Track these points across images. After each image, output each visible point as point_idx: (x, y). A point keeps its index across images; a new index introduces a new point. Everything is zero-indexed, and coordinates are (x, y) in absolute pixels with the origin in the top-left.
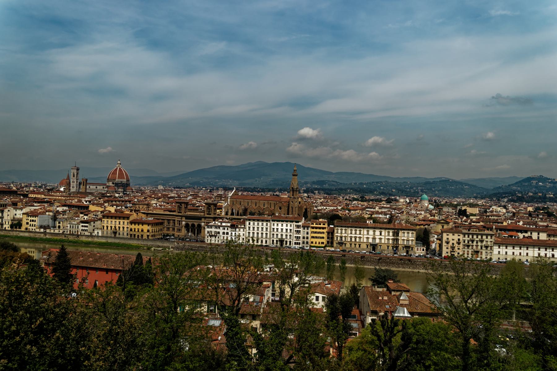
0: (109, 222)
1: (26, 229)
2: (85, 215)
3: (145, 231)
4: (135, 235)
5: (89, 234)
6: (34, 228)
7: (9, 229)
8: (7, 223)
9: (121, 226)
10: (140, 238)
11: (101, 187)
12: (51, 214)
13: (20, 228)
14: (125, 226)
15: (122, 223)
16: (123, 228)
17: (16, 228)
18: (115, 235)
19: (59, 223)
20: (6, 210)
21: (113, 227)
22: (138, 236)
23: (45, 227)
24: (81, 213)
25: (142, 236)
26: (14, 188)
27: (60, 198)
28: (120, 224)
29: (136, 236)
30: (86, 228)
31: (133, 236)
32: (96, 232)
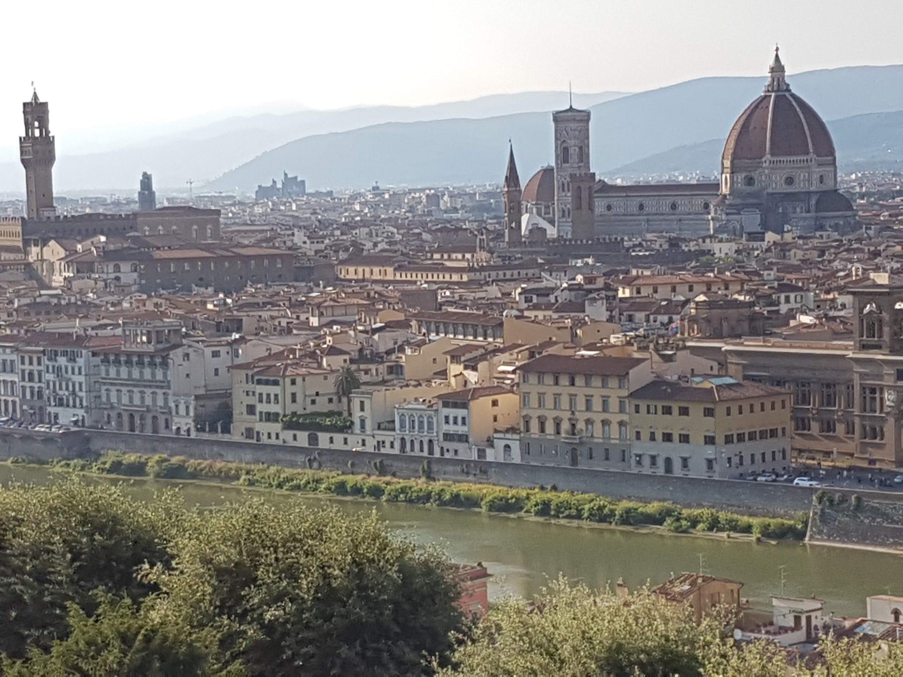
0: (549, 402)
1: (249, 432)
2: (466, 368)
3: (697, 438)
4: (653, 458)
5: (474, 456)
6: (276, 427)
7: (193, 435)
8: (182, 408)
9: (598, 418)
10: (678, 471)
11: (699, 202)
12: (338, 362)
13: (229, 432)
14: (615, 418)
15: (597, 405)
16: (605, 423)
17: (213, 430)
18: (574, 461)
19: (362, 409)
20: (176, 356)
21: (565, 426)
22: (668, 461)
23: (312, 424)
24: (455, 357)
25: (685, 461)
26: (299, 238)
27: (455, 278)
28: (588, 408)
29: (661, 462)
30: (461, 429)
31: (646, 461)
32: (500, 444)
